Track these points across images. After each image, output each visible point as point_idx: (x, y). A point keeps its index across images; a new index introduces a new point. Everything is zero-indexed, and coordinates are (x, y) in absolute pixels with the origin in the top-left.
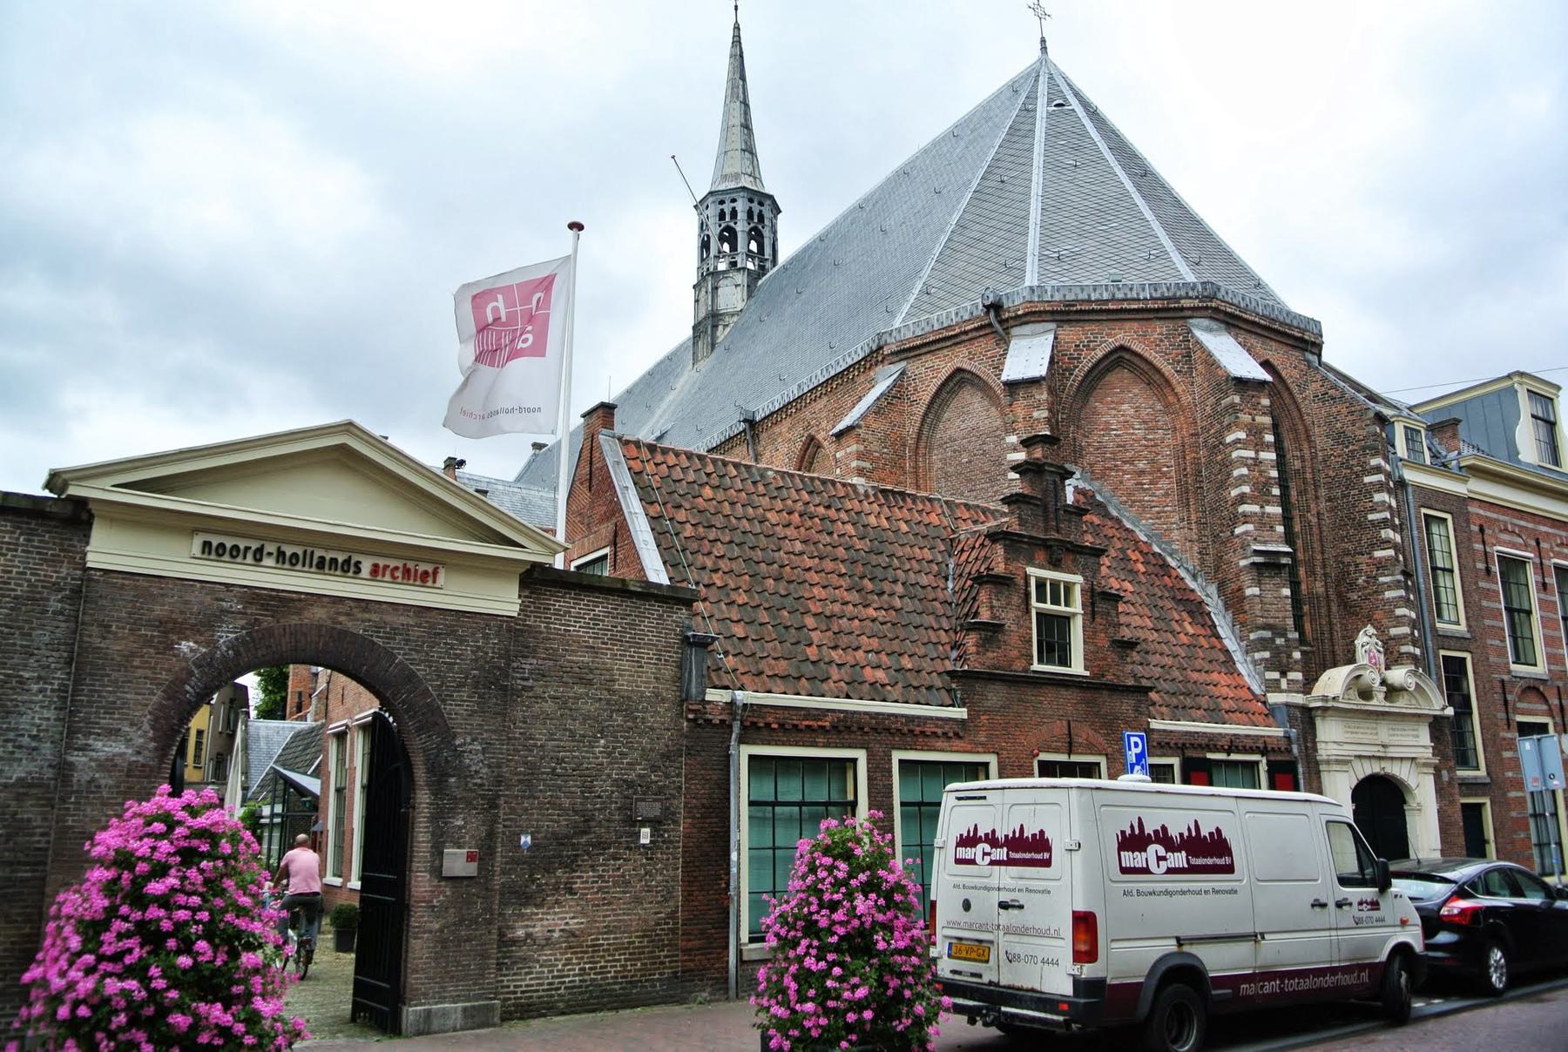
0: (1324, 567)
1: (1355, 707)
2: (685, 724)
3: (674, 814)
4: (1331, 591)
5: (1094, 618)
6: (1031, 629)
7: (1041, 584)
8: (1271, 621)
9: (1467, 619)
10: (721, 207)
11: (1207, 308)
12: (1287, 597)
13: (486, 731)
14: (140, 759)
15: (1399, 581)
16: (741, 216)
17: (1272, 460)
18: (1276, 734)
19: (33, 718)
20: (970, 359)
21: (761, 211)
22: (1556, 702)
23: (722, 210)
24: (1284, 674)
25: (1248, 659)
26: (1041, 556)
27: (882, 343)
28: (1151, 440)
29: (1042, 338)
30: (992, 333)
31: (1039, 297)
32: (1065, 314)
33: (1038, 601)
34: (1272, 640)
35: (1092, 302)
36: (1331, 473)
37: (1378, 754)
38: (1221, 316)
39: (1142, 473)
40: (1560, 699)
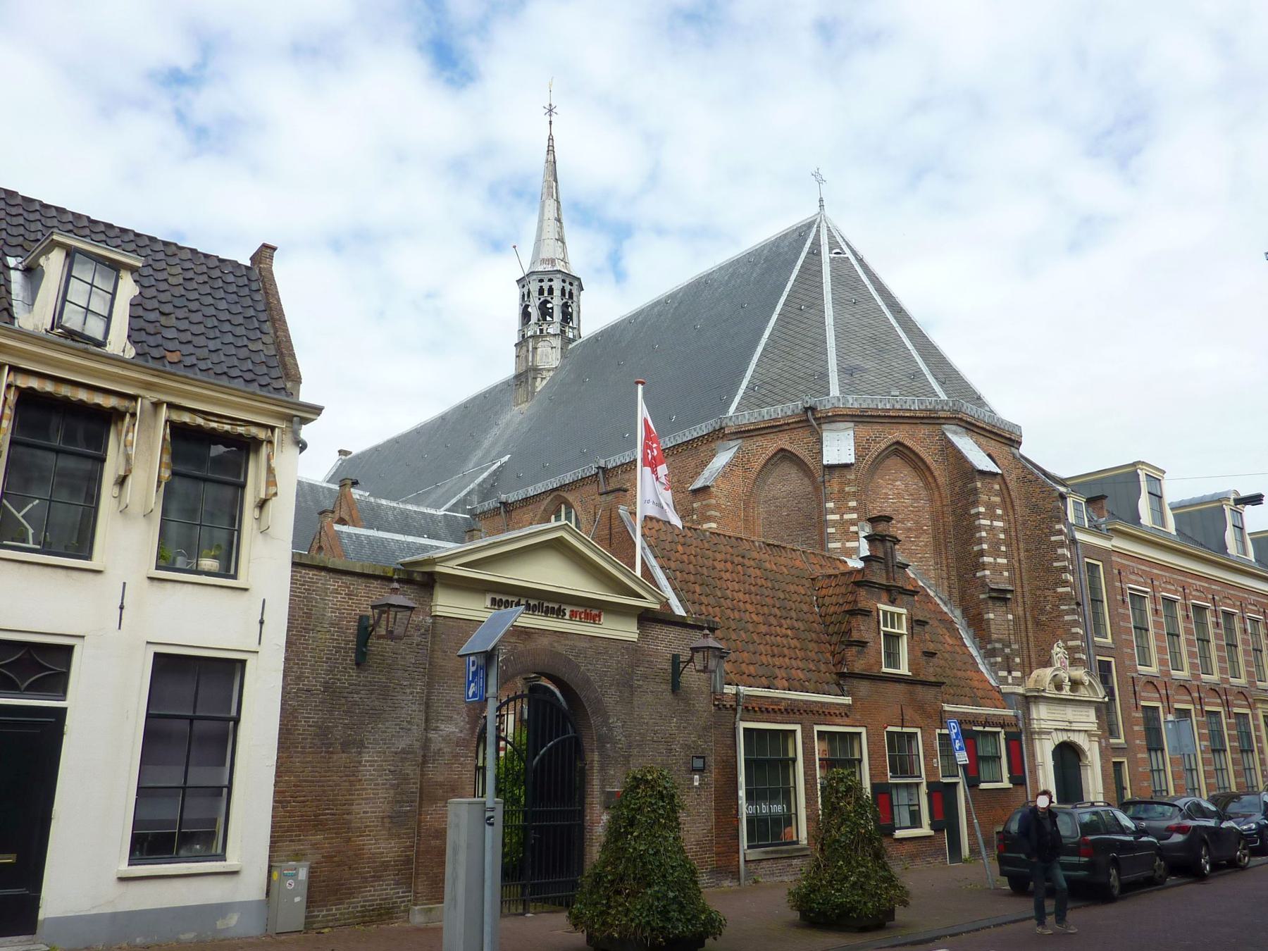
0: (1023, 597)
1: (1054, 696)
2: (713, 708)
3: (709, 766)
4: (1028, 614)
5: (912, 637)
6: (881, 644)
7: (885, 613)
8: (1001, 636)
9: (1112, 635)
10: (540, 284)
11: (955, 418)
12: (1011, 620)
13: (624, 714)
14: (462, 735)
15: (1074, 609)
16: (557, 293)
17: (1001, 527)
18: (1009, 714)
19: (408, 710)
20: (790, 443)
21: (571, 290)
22: (1164, 692)
23: (541, 287)
24: (1010, 673)
25: (986, 662)
26: (884, 596)
27: (723, 425)
28: (914, 507)
29: (846, 433)
30: (808, 426)
31: (843, 404)
32: (860, 418)
33: (884, 626)
34: (1003, 650)
35: (879, 410)
36: (1028, 533)
37: (1066, 728)
39: (910, 529)
40: (1166, 690)
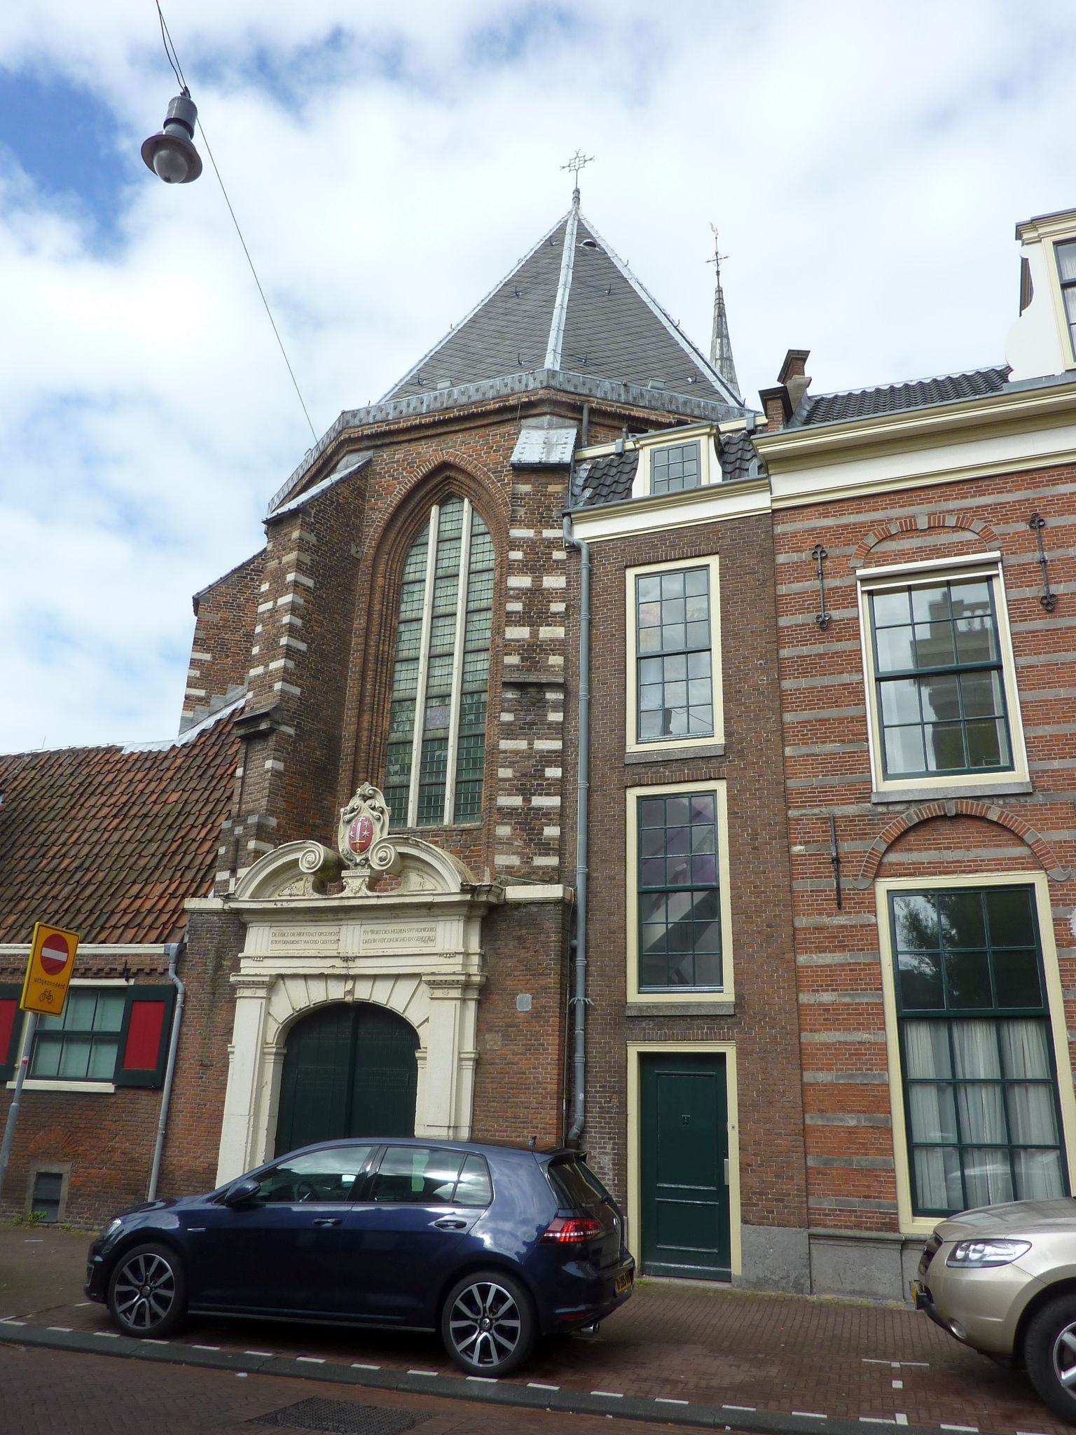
34: (232, 830)
37: (326, 972)
38: (366, 443)
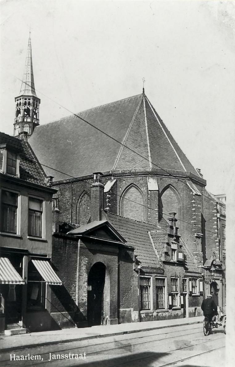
23: (26, 102)
